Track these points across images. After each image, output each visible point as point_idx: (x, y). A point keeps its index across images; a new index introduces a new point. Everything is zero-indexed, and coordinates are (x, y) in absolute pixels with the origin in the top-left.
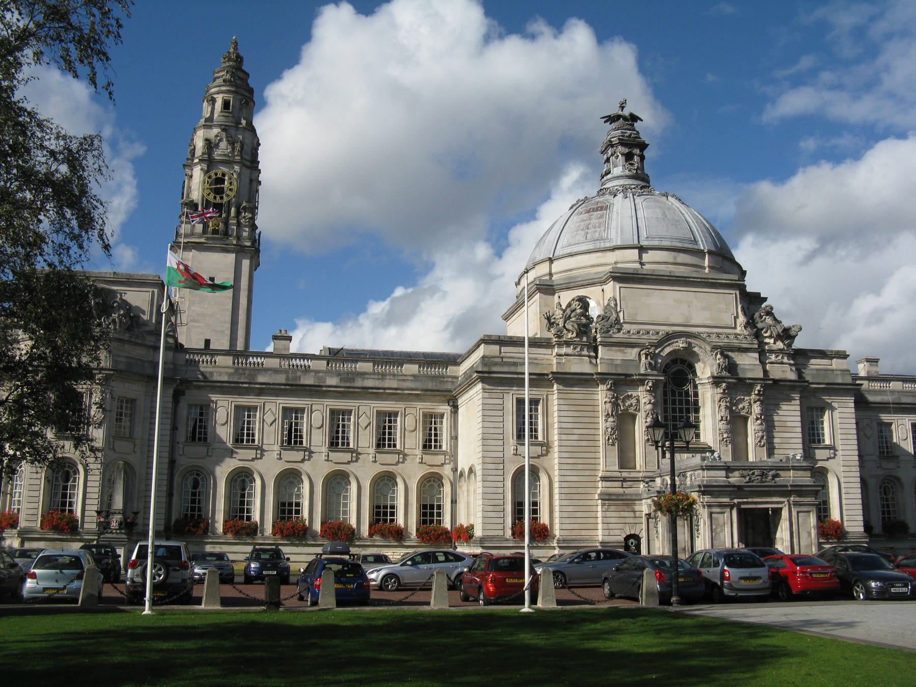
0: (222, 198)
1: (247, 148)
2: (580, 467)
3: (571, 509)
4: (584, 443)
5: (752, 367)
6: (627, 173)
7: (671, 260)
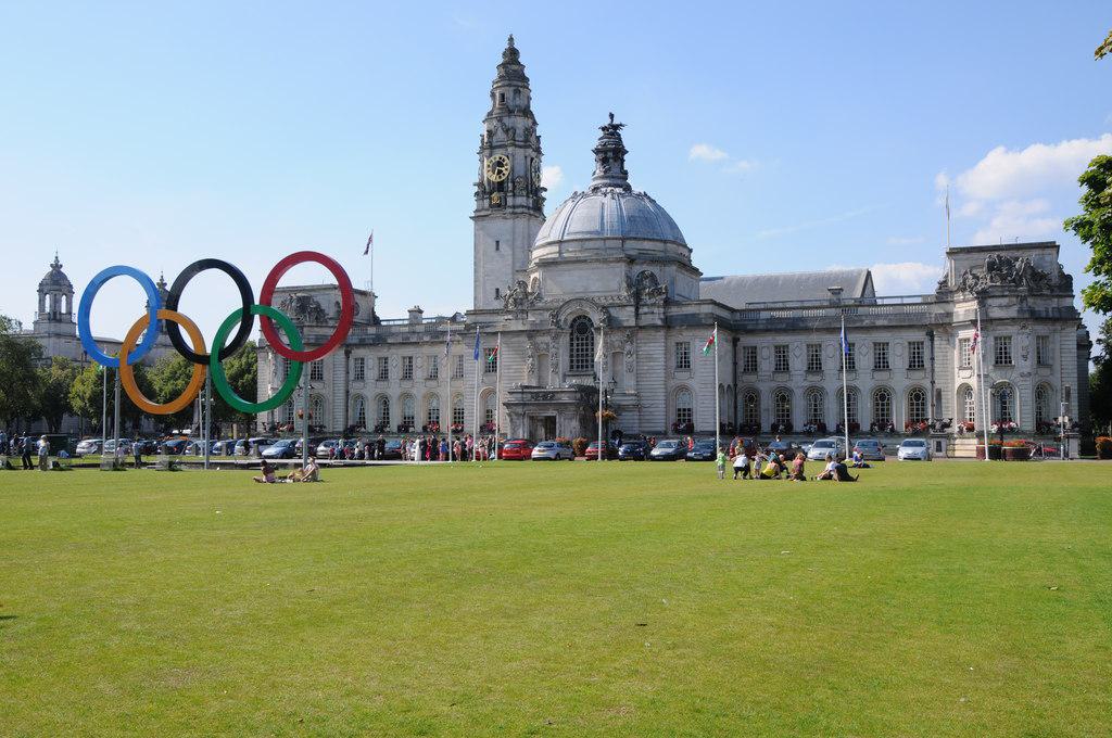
1: (520, 132)
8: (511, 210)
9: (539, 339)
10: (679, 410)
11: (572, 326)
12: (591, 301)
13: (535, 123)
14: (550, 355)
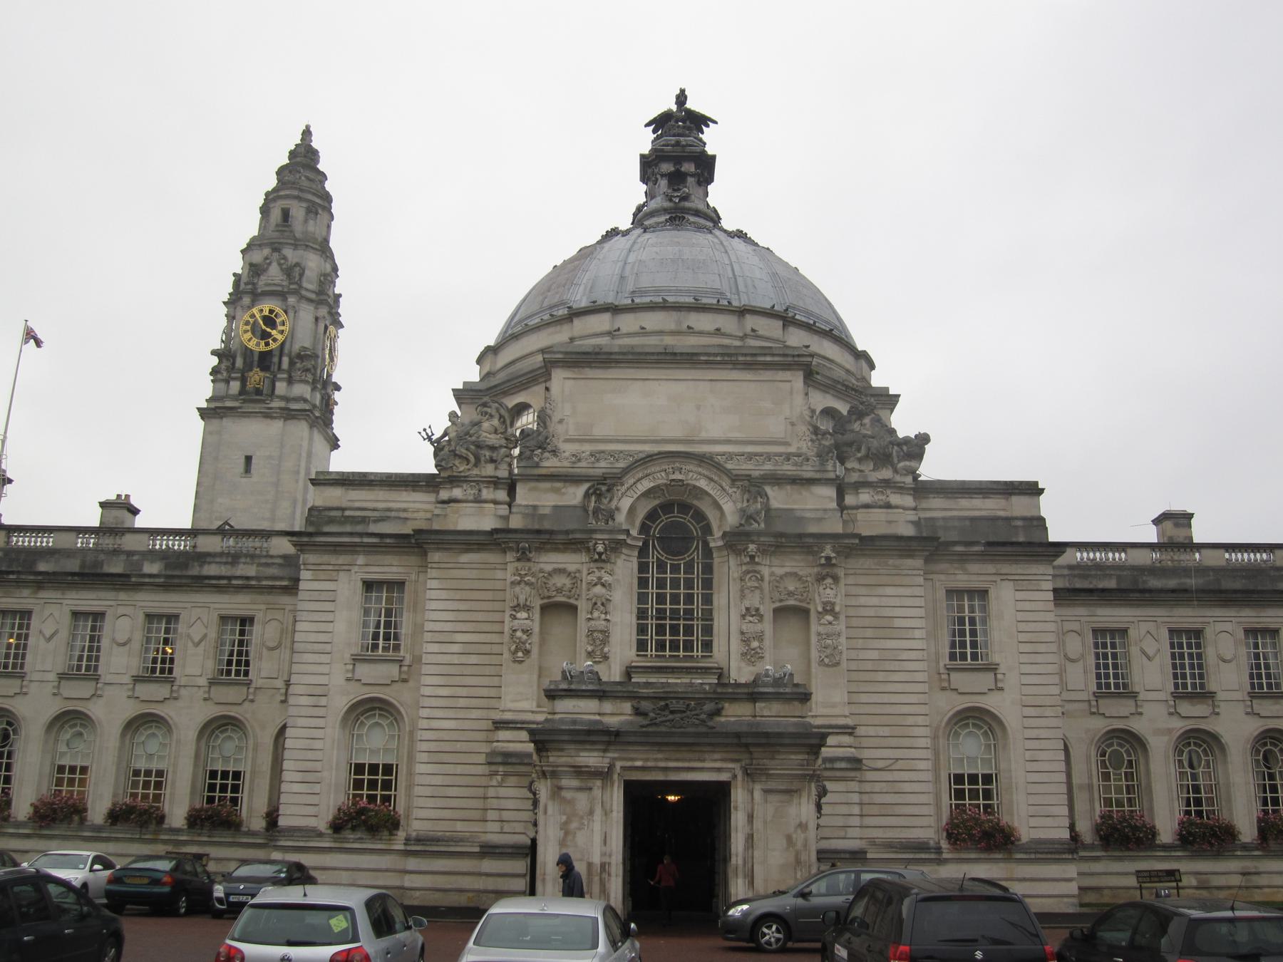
0: (267, 344)
2: (462, 703)
3: (438, 780)
4: (473, 659)
5: (819, 514)
6: (667, 204)
7: (673, 327)
8: (282, 404)
9: (549, 561)
10: (959, 779)
11: (644, 528)
12: (702, 459)
13: (335, 269)
14: (583, 606)
